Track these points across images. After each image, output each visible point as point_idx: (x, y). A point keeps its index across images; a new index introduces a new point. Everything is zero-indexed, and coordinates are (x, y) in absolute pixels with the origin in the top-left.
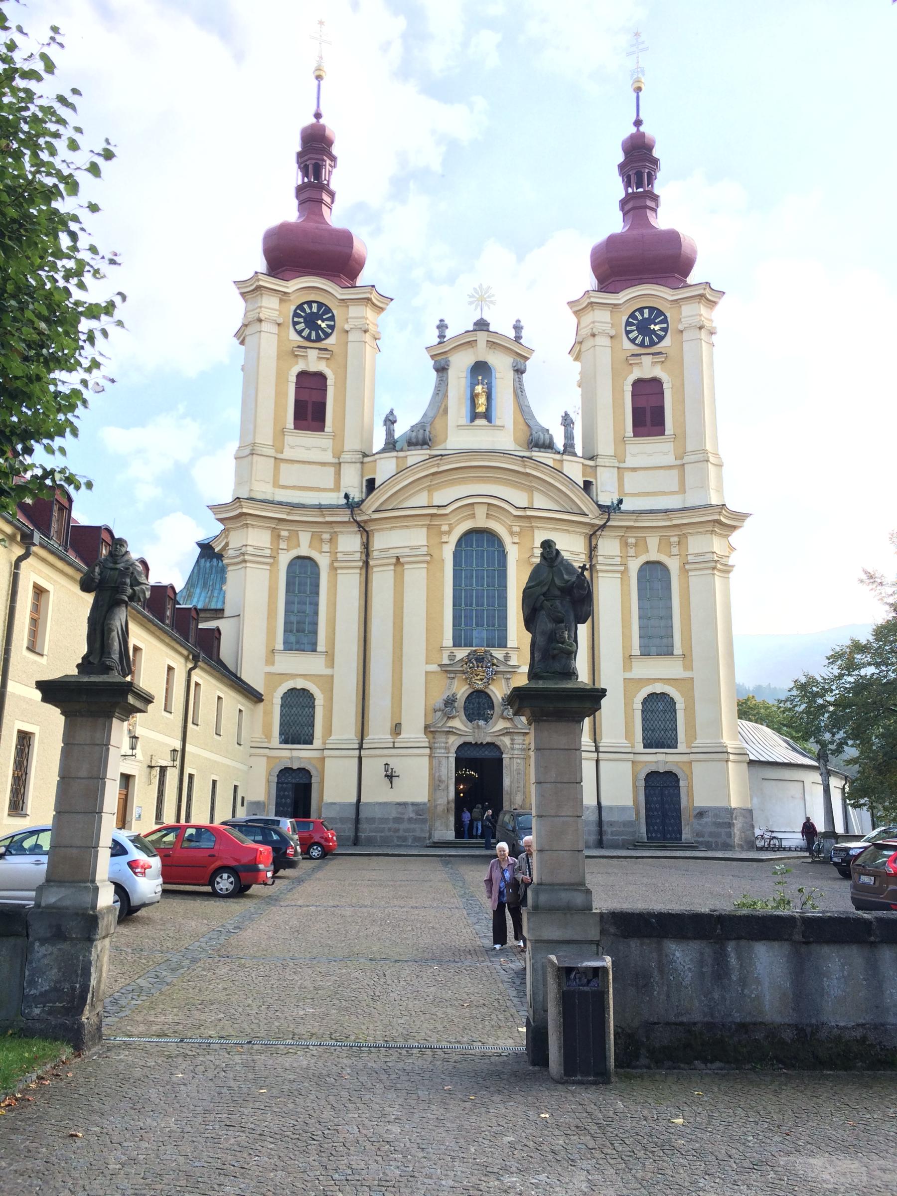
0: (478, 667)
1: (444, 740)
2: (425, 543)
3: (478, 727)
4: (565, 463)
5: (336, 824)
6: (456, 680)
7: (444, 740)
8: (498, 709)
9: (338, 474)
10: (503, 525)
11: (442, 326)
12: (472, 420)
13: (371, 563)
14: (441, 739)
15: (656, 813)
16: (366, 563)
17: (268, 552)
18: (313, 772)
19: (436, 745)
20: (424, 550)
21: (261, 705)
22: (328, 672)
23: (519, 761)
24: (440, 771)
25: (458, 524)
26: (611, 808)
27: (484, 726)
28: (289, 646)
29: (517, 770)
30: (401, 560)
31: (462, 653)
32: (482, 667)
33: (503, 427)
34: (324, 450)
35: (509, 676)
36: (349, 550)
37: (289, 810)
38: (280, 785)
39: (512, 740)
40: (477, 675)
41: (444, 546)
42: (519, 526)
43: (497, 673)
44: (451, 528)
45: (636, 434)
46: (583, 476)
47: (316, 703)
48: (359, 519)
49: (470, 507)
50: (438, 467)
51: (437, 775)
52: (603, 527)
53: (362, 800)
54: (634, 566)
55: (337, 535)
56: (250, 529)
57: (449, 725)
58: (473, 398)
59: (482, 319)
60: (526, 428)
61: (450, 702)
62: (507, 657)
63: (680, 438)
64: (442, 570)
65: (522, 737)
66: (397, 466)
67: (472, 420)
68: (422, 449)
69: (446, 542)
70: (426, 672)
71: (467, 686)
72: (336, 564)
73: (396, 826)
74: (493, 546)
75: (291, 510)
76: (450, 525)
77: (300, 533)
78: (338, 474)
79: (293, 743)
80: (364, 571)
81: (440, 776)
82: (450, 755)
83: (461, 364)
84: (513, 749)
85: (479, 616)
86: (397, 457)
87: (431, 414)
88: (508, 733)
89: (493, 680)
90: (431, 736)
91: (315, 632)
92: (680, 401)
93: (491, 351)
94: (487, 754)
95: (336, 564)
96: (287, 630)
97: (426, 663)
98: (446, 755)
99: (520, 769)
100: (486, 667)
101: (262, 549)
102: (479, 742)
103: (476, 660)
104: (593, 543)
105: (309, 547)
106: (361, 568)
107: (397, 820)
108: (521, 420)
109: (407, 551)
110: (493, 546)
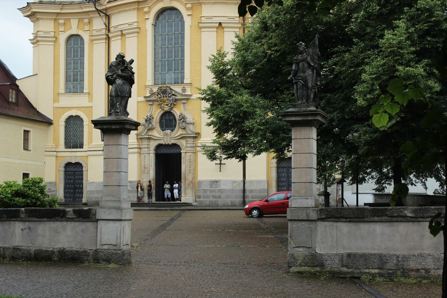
0: (164, 97)
1: (147, 143)
2: (136, 21)
3: (167, 135)
5: (95, 194)
6: (154, 106)
7: (147, 143)
8: (178, 122)
14: (145, 142)
15: (284, 184)
17: (52, 34)
18: (84, 165)
19: (143, 146)
20: (135, 25)
21: (52, 126)
22: (89, 105)
23: (190, 154)
24: (145, 162)
26: (251, 182)
27: (169, 133)
29: (189, 159)
30: (123, 32)
32: (166, 97)
35: (184, 101)
36: (99, 28)
37: (73, 186)
38: (67, 173)
39: (187, 141)
40: (164, 102)
41: (147, 21)
43: (176, 100)
47: (84, 123)
48: (99, 8)
51: (143, 164)
55: (92, 19)
56: (41, 21)
57: (149, 134)
62: (184, 90)
64: (146, 36)
65: (192, 140)
69: (147, 19)
70: (138, 102)
71: (160, 110)
72: (92, 38)
75: (63, 6)
77: (71, 20)
79: (73, 148)
80: (107, 42)
81: (145, 165)
82: (150, 152)
84: (187, 147)
85: (170, 64)
88: (183, 138)
89: (174, 105)
90: (140, 141)
94: (174, 151)
95: (92, 38)
96: (67, 79)
97: (138, 96)
98: (148, 152)
99: (191, 159)
100: (169, 97)
101: (48, 32)
102: (167, 144)
103: (162, 93)
105: (77, 28)
106: (106, 39)
109: (126, 27)
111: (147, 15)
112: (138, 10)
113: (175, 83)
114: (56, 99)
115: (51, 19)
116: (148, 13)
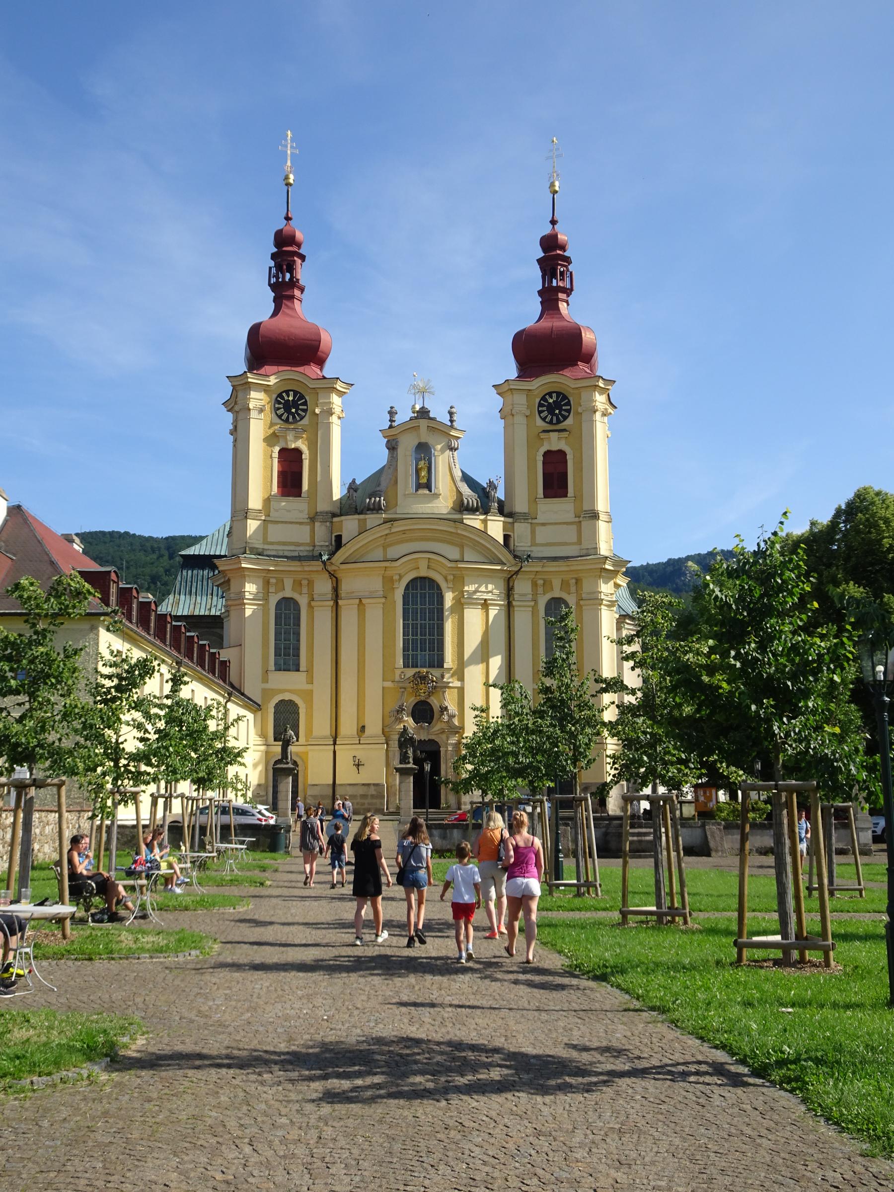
4: (489, 522)
9: (313, 531)
11: (392, 413)
12: (417, 490)
13: (340, 602)
16: (337, 603)
22: (309, 687)
28: (278, 668)
31: (410, 672)
34: (301, 512)
44: (401, 577)
45: (546, 496)
46: (504, 530)
48: (330, 569)
52: (517, 573)
53: (337, 782)
54: (542, 602)
58: (418, 471)
61: (400, 710)
63: (579, 497)
66: (359, 526)
67: (417, 490)
68: (378, 513)
73: (362, 801)
74: (433, 589)
78: (313, 531)
83: (407, 444)
85: (423, 642)
86: (359, 520)
91: (298, 656)
92: (579, 468)
96: (277, 654)
103: (420, 677)
104: (511, 584)
107: (364, 796)
110: (433, 589)
113: (430, 667)
114: (265, 680)
115: (259, 577)
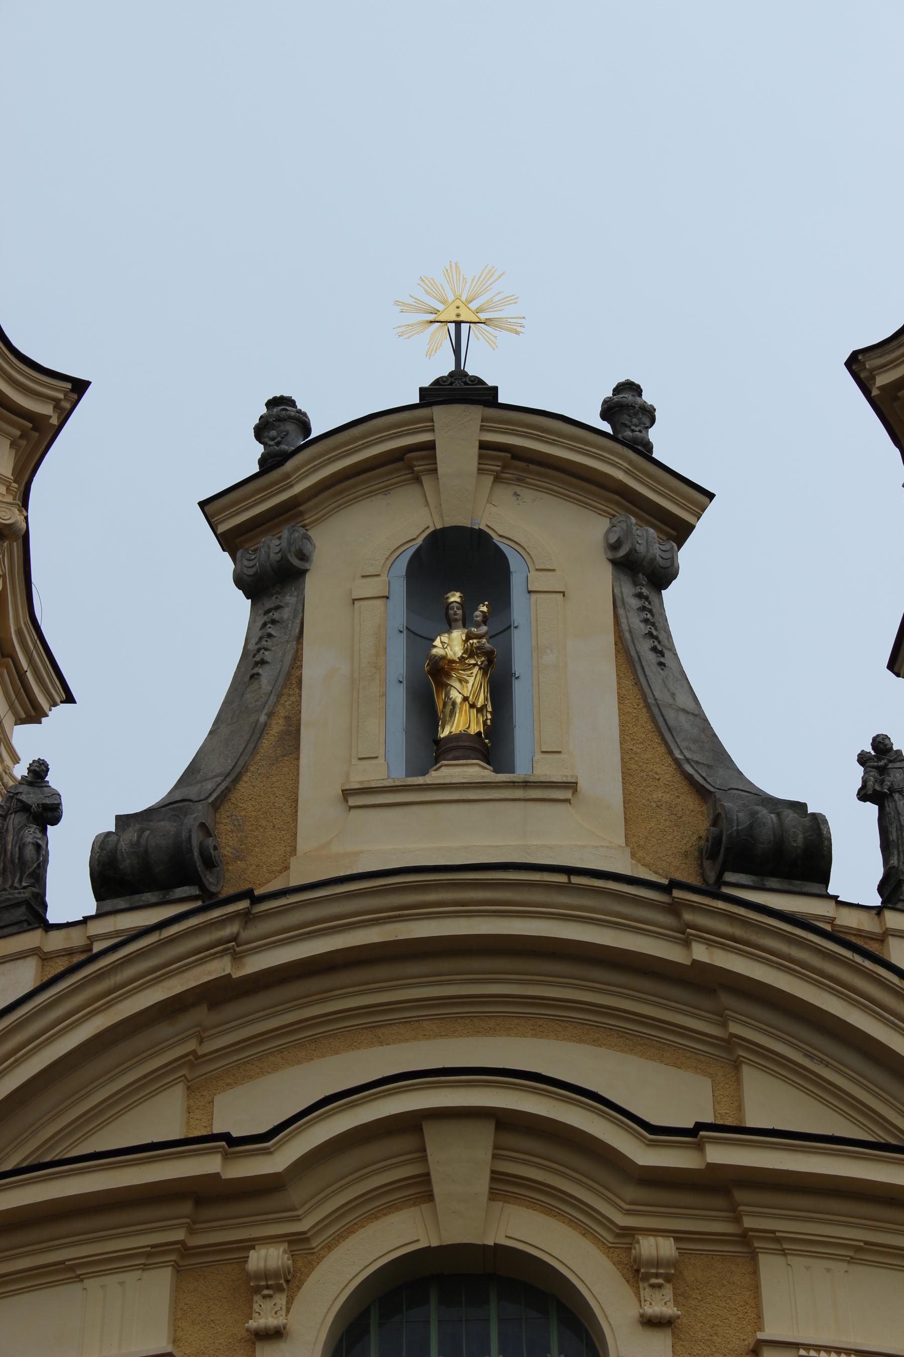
10: (586, 1232)
25: (341, 1237)
33: (572, 786)
42: (679, 1237)
49: (403, 1143)
50: (237, 957)
59: (459, 374)
60: (689, 802)
69: (275, 1335)
76: (296, 1241)
86: (45, 957)
87: (219, 765)
93: (504, 493)
108: (666, 771)
111: (267, 1305)
112: (178, 1269)
116: (279, 1289)
